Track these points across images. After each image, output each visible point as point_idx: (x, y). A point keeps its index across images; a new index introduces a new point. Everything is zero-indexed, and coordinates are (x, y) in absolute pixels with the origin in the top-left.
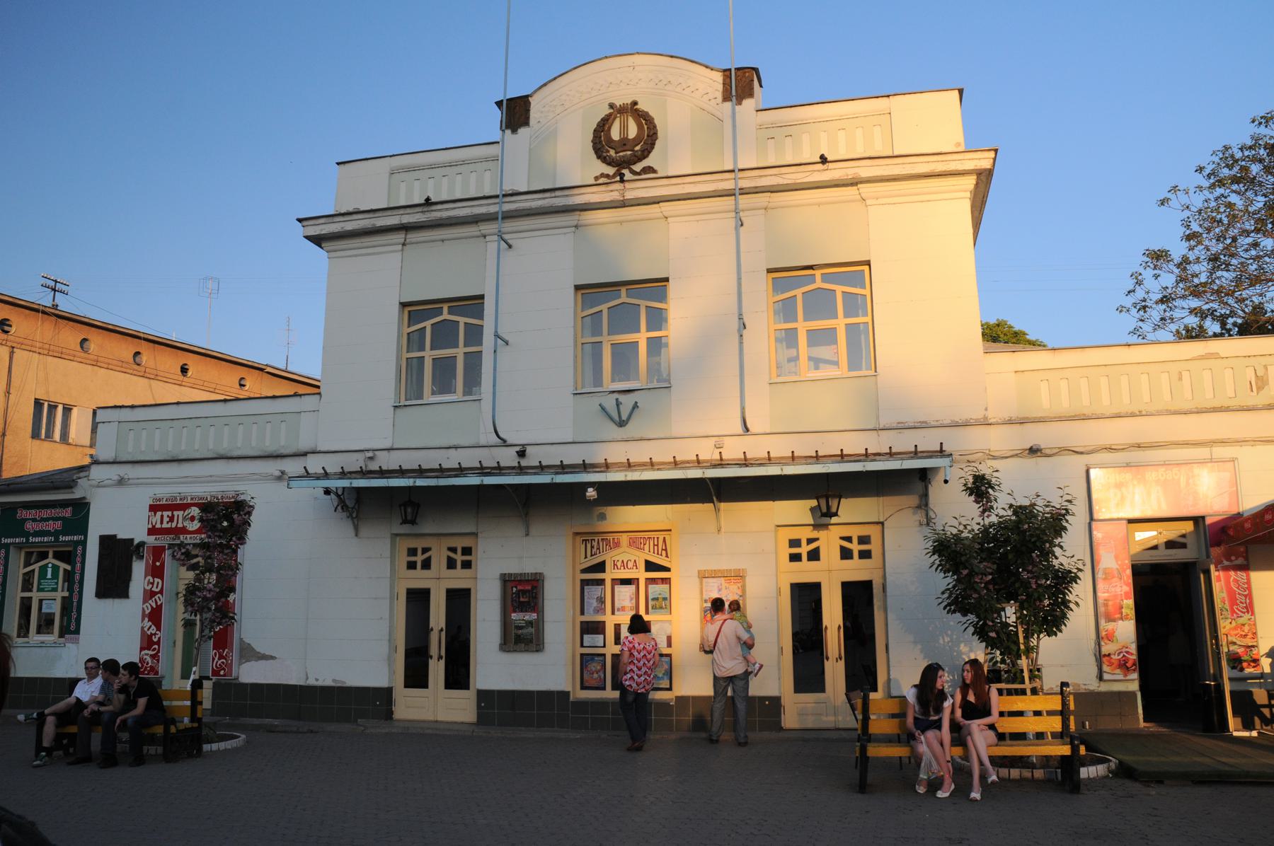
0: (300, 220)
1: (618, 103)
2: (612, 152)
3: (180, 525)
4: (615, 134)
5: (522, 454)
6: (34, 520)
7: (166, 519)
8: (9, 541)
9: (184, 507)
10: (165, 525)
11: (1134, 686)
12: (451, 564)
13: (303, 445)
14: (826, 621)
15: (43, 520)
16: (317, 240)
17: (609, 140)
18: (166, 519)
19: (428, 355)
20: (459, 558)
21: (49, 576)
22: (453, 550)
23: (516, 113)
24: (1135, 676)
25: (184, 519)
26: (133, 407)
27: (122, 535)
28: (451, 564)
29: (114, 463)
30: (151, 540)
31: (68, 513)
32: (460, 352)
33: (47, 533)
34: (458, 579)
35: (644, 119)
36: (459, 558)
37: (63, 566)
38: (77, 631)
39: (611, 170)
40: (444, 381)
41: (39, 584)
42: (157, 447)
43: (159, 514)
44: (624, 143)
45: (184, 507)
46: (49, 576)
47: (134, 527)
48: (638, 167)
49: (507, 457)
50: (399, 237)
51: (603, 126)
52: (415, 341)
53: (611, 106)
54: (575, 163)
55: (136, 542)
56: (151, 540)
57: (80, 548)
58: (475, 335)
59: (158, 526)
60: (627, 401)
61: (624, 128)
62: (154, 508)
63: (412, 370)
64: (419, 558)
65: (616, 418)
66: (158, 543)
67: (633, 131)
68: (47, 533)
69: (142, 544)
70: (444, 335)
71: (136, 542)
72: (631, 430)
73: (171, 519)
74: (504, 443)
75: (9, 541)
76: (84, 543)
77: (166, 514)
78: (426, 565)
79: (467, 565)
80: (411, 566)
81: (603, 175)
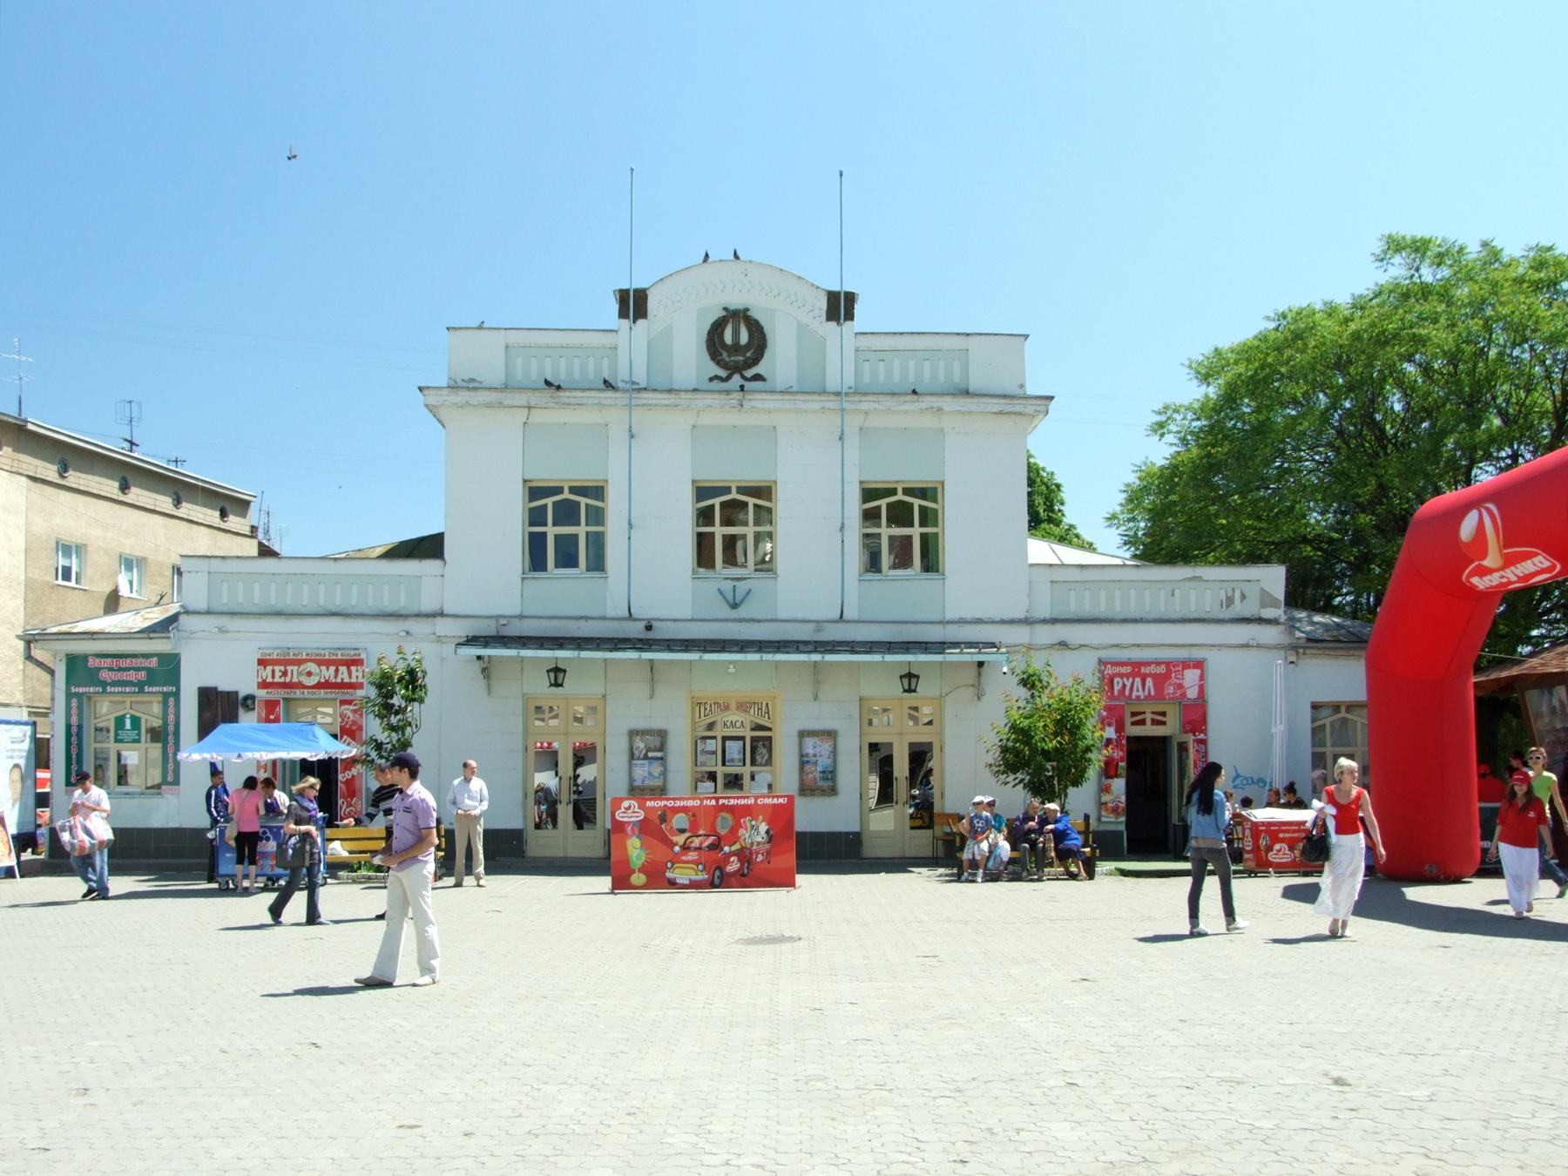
0: (420, 389)
1: (732, 308)
2: (725, 355)
3: (295, 680)
5: (649, 628)
6: (111, 669)
7: (278, 674)
8: (81, 690)
9: (299, 662)
10: (277, 680)
11: (1122, 827)
13: (428, 605)
14: (896, 773)
15: (120, 669)
17: (724, 345)
18: (278, 674)
21: (128, 726)
23: (633, 304)
24: (1123, 819)
25: (300, 674)
26: (223, 558)
27: (224, 686)
29: (208, 613)
30: (262, 694)
33: (129, 684)
35: (757, 330)
38: (176, 782)
39: (723, 373)
41: (116, 735)
42: (257, 600)
43: (269, 668)
44: (736, 348)
45: (299, 662)
46: (128, 726)
47: (241, 678)
48: (749, 373)
51: (717, 329)
53: (725, 309)
54: (689, 358)
55: (241, 695)
56: (262, 694)
57: (171, 700)
58: (597, 516)
59: (269, 680)
61: (736, 334)
62: (262, 662)
63: (536, 546)
65: (730, 597)
66: (271, 697)
67: (744, 338)
68: (129, 684)
69: (251, 698)
70: (567, 513)
71: (241, 695)
72: (743, 612)
73: (285, 674)
75: (81, 690)
76: (177, 695)
77: (277, 668)
81: (717, 377)
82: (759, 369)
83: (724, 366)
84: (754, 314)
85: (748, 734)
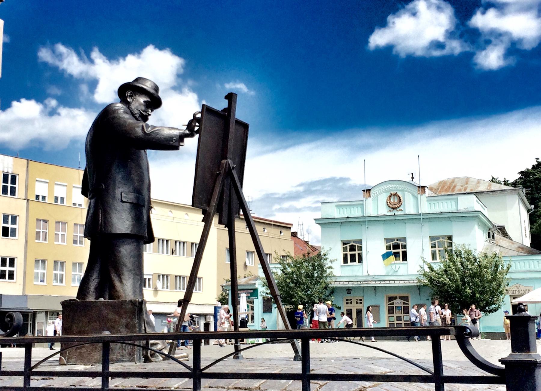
4: (392, 200)
12: (357, 303)
16: (319, 224)
19: (349, 253)
20: (359, 301)
22: (358, 300)
28: (357, 303)
31: (252, 291)
32: (356, 253)
34: (359, 306)
36: (359, 301)
37: (250, 305)
39: (392, 210)
40: (353, 259)
48: (398, 209)
49: (370, 279)
50: (340, 224)
52: (345, 249)
60: (398, 266)
64: (349, 302)
74: (369, 276)
78: (351, 303)
79: (361, 303)
80: (347, 303)
82: (401, 208)
83: (392, 208)
84: (399, 194)
85: (402, 305)
